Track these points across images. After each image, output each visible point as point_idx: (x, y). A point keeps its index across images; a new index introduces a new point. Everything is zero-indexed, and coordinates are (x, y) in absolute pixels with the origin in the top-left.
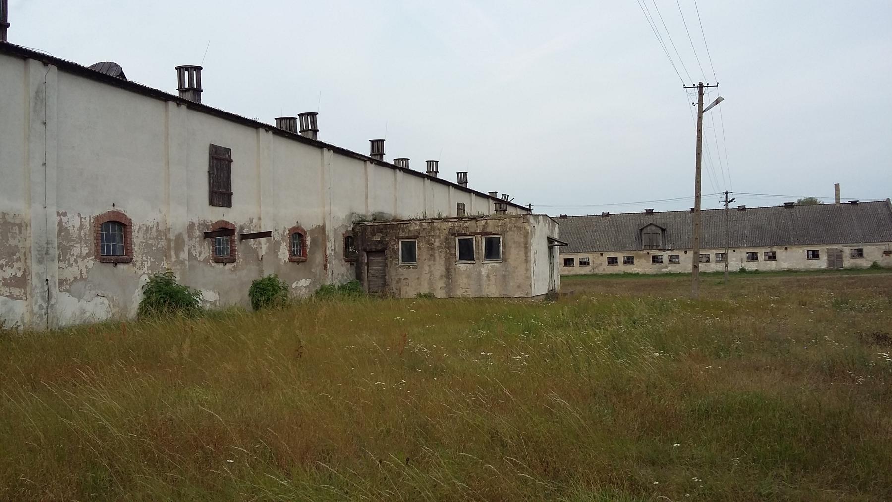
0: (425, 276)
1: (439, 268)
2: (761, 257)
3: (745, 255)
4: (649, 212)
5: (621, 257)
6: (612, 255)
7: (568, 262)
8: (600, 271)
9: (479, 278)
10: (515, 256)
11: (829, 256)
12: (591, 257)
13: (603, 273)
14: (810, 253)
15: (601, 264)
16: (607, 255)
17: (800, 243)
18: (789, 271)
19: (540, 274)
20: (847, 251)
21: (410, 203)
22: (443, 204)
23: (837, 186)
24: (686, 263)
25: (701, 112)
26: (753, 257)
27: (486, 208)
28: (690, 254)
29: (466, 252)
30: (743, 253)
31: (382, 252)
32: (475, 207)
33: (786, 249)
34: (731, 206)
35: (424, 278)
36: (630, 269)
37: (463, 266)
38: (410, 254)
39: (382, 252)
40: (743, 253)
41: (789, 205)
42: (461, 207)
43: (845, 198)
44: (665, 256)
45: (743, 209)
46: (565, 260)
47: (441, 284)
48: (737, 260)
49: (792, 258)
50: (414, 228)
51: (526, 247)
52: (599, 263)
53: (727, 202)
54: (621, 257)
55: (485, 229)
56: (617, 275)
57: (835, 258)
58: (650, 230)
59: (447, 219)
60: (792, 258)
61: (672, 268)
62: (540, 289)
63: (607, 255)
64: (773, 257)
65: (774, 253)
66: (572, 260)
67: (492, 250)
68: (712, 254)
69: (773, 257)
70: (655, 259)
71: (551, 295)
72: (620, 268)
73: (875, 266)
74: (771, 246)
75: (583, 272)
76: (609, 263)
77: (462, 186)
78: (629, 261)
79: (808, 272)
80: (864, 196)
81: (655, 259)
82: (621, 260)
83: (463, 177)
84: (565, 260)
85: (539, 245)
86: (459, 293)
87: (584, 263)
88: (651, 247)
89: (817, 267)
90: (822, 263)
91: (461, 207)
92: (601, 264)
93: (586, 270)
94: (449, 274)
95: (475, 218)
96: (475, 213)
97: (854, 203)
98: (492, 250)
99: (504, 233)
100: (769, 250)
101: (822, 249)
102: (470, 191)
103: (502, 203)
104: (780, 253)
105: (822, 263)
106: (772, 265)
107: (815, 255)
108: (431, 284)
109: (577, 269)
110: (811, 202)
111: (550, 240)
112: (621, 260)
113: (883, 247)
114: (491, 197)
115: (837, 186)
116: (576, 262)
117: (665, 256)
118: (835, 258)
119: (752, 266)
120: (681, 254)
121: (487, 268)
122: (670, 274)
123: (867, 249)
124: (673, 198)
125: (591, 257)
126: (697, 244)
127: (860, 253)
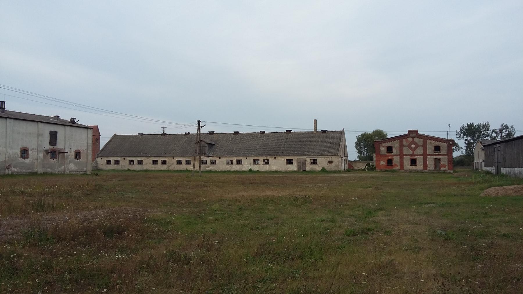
2: (261, 163)
3: (252, 161)
5: (184, 160)
6: (179, 158)
11: (298, 163)
13: (174, 169)
14: (312, 161)
15: (173, 164)
16: (177, 159)
17: (283, 155)
18: (276, 172)
20: (309, 160)
23: (315, 121)
33: (275, 158)
34: (203, 131)
43: (320, 129)
46: (287, 160)
49: (278, 164)
53: (199, 127)
54: (184, 160)
56: (181, 171)
60: (278, 164)
63: (177, 159)
64: (267, 163)
65: (268, 160)
66: (157, 161)
69: (267, 163)
72: (184, 167)
74: (266, 156)
75: (162, 169)
76: (178, 163)
79: (287, 172)
80: (329, 129)
82: (184, 162)
84: (287, 160)
87: (164, 163)
89: (291, 169)
92: (173, 164)
93: (164, 167)
94: (200, 167)
97: (324, 131)
100: (265, 158)
101: (295, 159)
104: (271, 160)
105: (294, 167)
106: (267, 168)
107: (290, 162)
113: (328, 159)
115: (315, 121)
116: (159, 162)
118: (302, 164)
119: (255, 168)
120: (217, 159)
122: (210, 172)
123: (320, 160)
127: (314, 162)
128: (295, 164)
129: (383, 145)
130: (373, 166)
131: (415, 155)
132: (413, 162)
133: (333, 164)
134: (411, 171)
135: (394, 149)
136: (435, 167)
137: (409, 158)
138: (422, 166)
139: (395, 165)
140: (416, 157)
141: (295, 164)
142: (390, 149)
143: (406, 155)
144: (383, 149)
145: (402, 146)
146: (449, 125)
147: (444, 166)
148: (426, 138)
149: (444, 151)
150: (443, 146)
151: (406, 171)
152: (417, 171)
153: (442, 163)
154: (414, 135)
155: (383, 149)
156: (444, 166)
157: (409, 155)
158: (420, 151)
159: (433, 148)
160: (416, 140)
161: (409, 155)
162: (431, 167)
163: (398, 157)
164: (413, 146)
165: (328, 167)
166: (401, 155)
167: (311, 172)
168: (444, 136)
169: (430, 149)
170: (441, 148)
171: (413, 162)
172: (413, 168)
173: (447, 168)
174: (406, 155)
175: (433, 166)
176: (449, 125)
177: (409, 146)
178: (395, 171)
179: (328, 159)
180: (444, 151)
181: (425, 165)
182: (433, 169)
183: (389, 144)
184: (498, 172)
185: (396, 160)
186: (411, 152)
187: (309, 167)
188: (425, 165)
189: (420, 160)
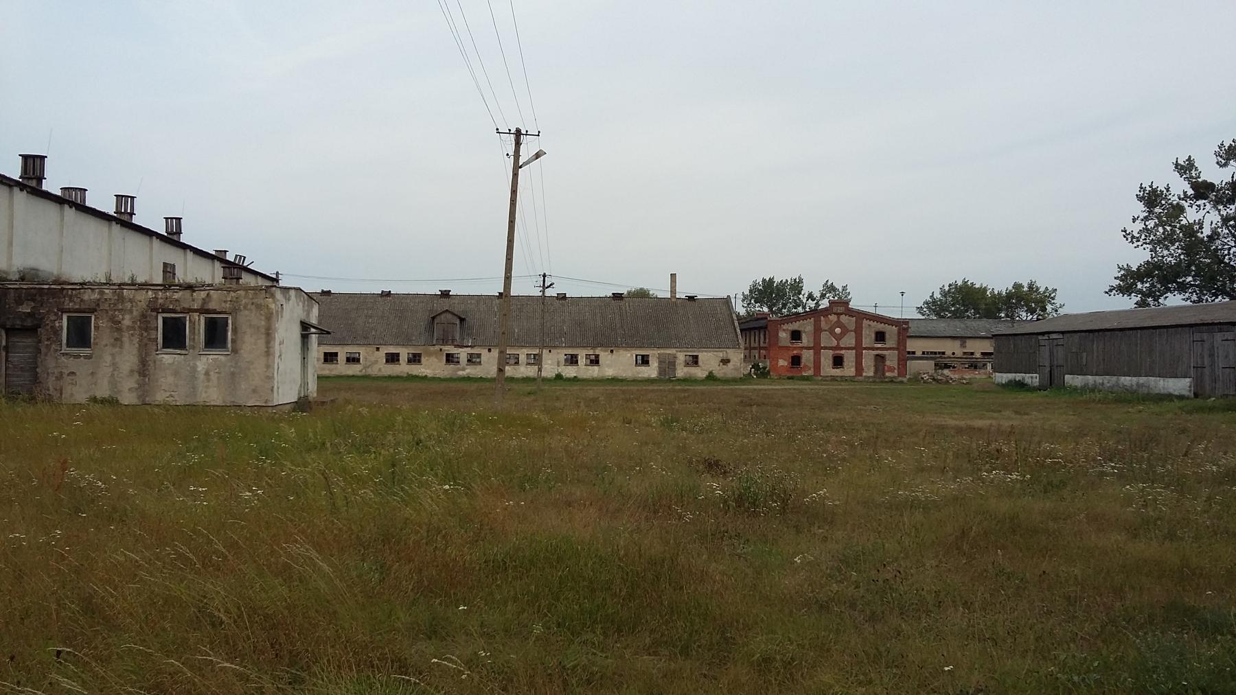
0: (105, 370)
1: (129, 358)
2: (582, 361)
3: (562, 358)
4: (445, 294)
5: (404, 353)
6: (392, 350)
7: (330, 358)
8: (374, 371)
9: (193, 376)
10: (250, 345)
11: (660, 362)
12: (363, 352)
13: (380, 374)
15: (376, 362)
18: (614, 380)
19: (289, 374)
20: (681, 357)
21: (86, 258)
22: (141, 263)
23: (673, 276)
24: (489, 364)
25: (517, 167)
26: (573, 360)
27: (211, 274)
28: (495, 353)
29: (175, 336)
30: (561, 354)
31: (33, 330)
32: (191, 270)
34: (549, 292)
35: (104, 373)
36: (416, 370)
37: (168, 358)
38: (80, 336)
39: (33, 330)
40: (561, 354)
41: (617, 297)
42: (168, 269)
43: (681, 294)
44: (463, 354)
45: (563, 297)
47: (131, 383)
48: (553, 364)
49: (618, 364)
50: (90, 296)
51: (269, 334)
52: (373, 361)
53: (544, 287)
54: (404, 353)
55: (207, 304)
56: (398, 378)
57: (668, 365)
58: (446, 319)
59: (145, 286)
60: (618, 364)
61: (470, 371)
62: (286, 394)
64: (595, 361)
65: (597, 356)
66: (336, 354)
67: (216, 335)
68: (523, 354)
69: (595, 361)
70: (450, 359)
71: (302, 404)
72: (403, 368)
73: (711, 377)
74: (594, 348)
75: (350, 373)
76: (387, 361)
77: (172, 237)
78: (415, 359)
79: (635, 381)
80: (704, 291)
81: (450, 359)
82: (404, 358)
83: (175, 224)
85: (287, 332)
86: (160, 397)
87: (353, 360)
88: (444, 341)
89: (646, 375)
90: (652, 371)
91: (168, 269)
92: (376, 362)
93: (354, 369)
95: (190, 287)
96: (190, 279)
97: (691, 298)
98: (216, 335)
99: (234, 311)
100: (591, 352)
101: (653, 354)
102: (185, 247)
103: (234, 269)
104: (604, 356)
105: (652, 371)
106: (594, 372)
107: (645, 361)
108: (113, 383)
109: (341, 368)
110: (642, 294)
111: (305, 326)
112: (404, 358)
113: (721, 354)
114: (218, 257)
115: (673, 276)
116: (342, 357)
117: (463, 354)
118: (668, 365)
119: (570, 372)
120: (484, 352)
121: (206, 361)
122: (468, 379)
123: (703, 356)
124: (477, 278)
125: (363, 352)
126: (504, 341)
127: (695, 361)
128: (654, 364)
129: (785, 327)
130: (764, 368)
131: (842, 349)
132: (838, 361)
133: (730, 365)
134: (834, 379)
135: (804, 336)
136: (876, 372)
137: (831, 352)
138: (853, 369)
139: (806, 366)
140: (843, 352)
141: (654, 364)
142: (796, 335)
143: (825, 348)
144: (784, 336)
145: (818, 330)
146: (902, 294)
147: (891, 369)
148: (861, 316)
149: (891, 341)
150: (891, 331)
151: (825, 379)
152: (843, 379)
153: (888, 363)
154: (841, 309)
155: (784, 336)
156: (891, 369)
157: (831, 348)
158: (850, 340)
159: (873, 336)
160: (844, 319)
161: (831, 348)
162: (869, 372)
163: (811, 352)
164: (838, 330)
165: (719, 371)
166: (817, 348)
167: (686, 380)
168: (895, 315)
169: (868, 339)
170: (887, 336)
171: (838, 361)
172: (837, 372)
173: (896, 373)
174: (825, 348)
175: (873, 369)
176: (902, 294)
177: (832, 332)
178: (807, 379)
179: (721, 354)
180: (891, 341)
181: (859, 368)
182: (872, 374)
183: (795, 326)
184: (1052, 382)
185: (808, 356)
186: (834, 343)
187: (681, 372)
188: (859, 368)
189: (849, 357)
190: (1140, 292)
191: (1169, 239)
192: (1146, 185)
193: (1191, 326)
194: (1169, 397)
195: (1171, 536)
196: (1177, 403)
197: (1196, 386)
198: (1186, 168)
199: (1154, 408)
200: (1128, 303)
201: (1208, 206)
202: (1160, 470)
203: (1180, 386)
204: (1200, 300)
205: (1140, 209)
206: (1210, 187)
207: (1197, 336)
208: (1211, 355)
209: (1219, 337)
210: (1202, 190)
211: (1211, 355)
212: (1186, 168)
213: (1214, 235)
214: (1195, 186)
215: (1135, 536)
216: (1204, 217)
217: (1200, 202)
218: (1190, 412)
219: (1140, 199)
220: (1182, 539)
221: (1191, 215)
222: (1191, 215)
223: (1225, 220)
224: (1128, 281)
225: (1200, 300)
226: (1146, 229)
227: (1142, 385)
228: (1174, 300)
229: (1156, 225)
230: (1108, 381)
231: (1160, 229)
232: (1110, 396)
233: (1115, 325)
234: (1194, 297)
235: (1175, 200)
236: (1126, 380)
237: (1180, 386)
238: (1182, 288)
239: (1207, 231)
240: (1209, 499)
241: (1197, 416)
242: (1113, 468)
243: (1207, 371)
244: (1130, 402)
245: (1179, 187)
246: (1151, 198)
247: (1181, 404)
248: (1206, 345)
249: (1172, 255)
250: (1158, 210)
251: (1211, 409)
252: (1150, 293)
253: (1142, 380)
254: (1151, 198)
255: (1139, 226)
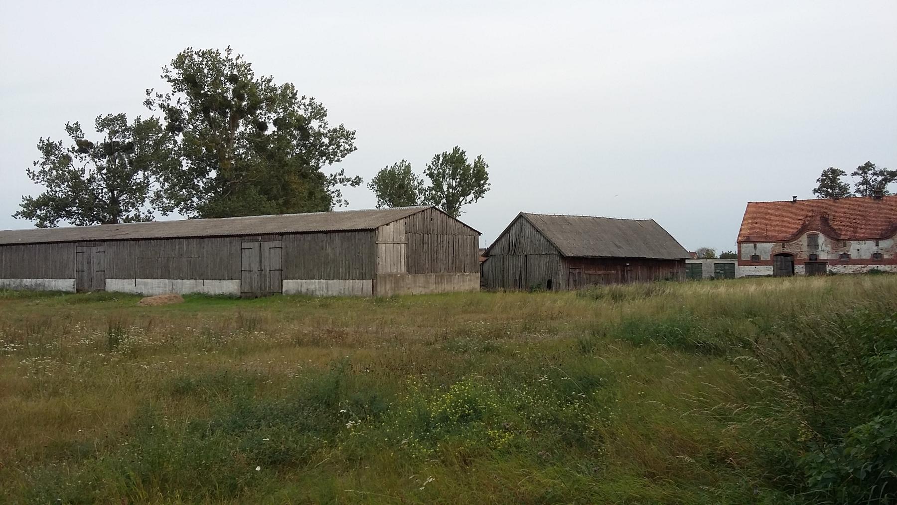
190: (38, 217)
191: (61, 179)
192: (45, 139)
193: (74, 242)
194: (59, 293)
195: (55, 393)
196: (64, 297)
197: (78, 284)
198: (74, 130)
199: (48, 301)
200: (30, 225)
201: (88, 159)
202: (48, 346)
203: (66, 284)
204: (82, 224)
205: (40, 156)
206: (90, 145)
207: (79, 249)
208: (89, 263)
209: (94, 250)
210: (84, 147)
211: (89, 263)
212: (74, 130)
213: (92, 179)
214: (79, 143)
215: (28, 397)
216: (85, 165)
217: (83, 155)
218: (73, 303)
219: (40, 149)
220: (63, 394)
221: (77, 164)
222: (77, 164)
223: (100, 169)
224: (30, 208)
225: (82, 224)
226: (43, 172)
227: (40, 285)
228: (63, 223)
229: (51, 169)
230: (13, 282)
231: (54, 172)
232: (16, 294)
233: (20, 241)
234: (78, 222)
235: (65, 152)
236: (27, 282)
237: (66, 284)
238: (69, 215)
239: (87, 176)
240: (83, 363)
241: (77, 306)
242: (13, 348)
243: (85, 274)
244: (29, 297)
245: (68, 143)
246: (48, 149)
247: (68, 297)
248: (85, 255)
249: (62, 191)
250: (52, 158)
251: (88, 300)
252: (43, 219)
253: (39, 281)
254: (48, 149)
255: (37, 169)
